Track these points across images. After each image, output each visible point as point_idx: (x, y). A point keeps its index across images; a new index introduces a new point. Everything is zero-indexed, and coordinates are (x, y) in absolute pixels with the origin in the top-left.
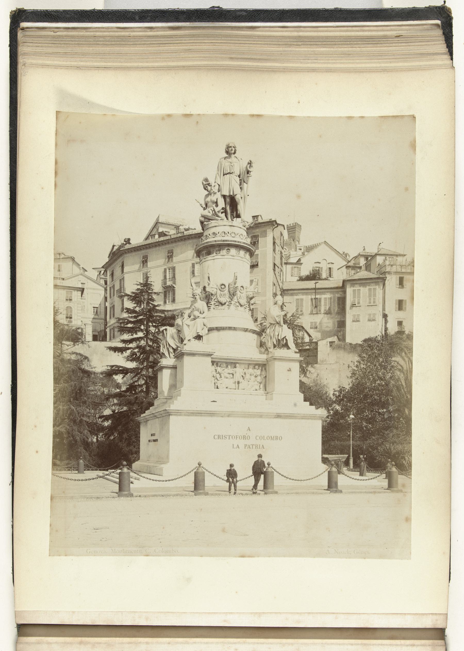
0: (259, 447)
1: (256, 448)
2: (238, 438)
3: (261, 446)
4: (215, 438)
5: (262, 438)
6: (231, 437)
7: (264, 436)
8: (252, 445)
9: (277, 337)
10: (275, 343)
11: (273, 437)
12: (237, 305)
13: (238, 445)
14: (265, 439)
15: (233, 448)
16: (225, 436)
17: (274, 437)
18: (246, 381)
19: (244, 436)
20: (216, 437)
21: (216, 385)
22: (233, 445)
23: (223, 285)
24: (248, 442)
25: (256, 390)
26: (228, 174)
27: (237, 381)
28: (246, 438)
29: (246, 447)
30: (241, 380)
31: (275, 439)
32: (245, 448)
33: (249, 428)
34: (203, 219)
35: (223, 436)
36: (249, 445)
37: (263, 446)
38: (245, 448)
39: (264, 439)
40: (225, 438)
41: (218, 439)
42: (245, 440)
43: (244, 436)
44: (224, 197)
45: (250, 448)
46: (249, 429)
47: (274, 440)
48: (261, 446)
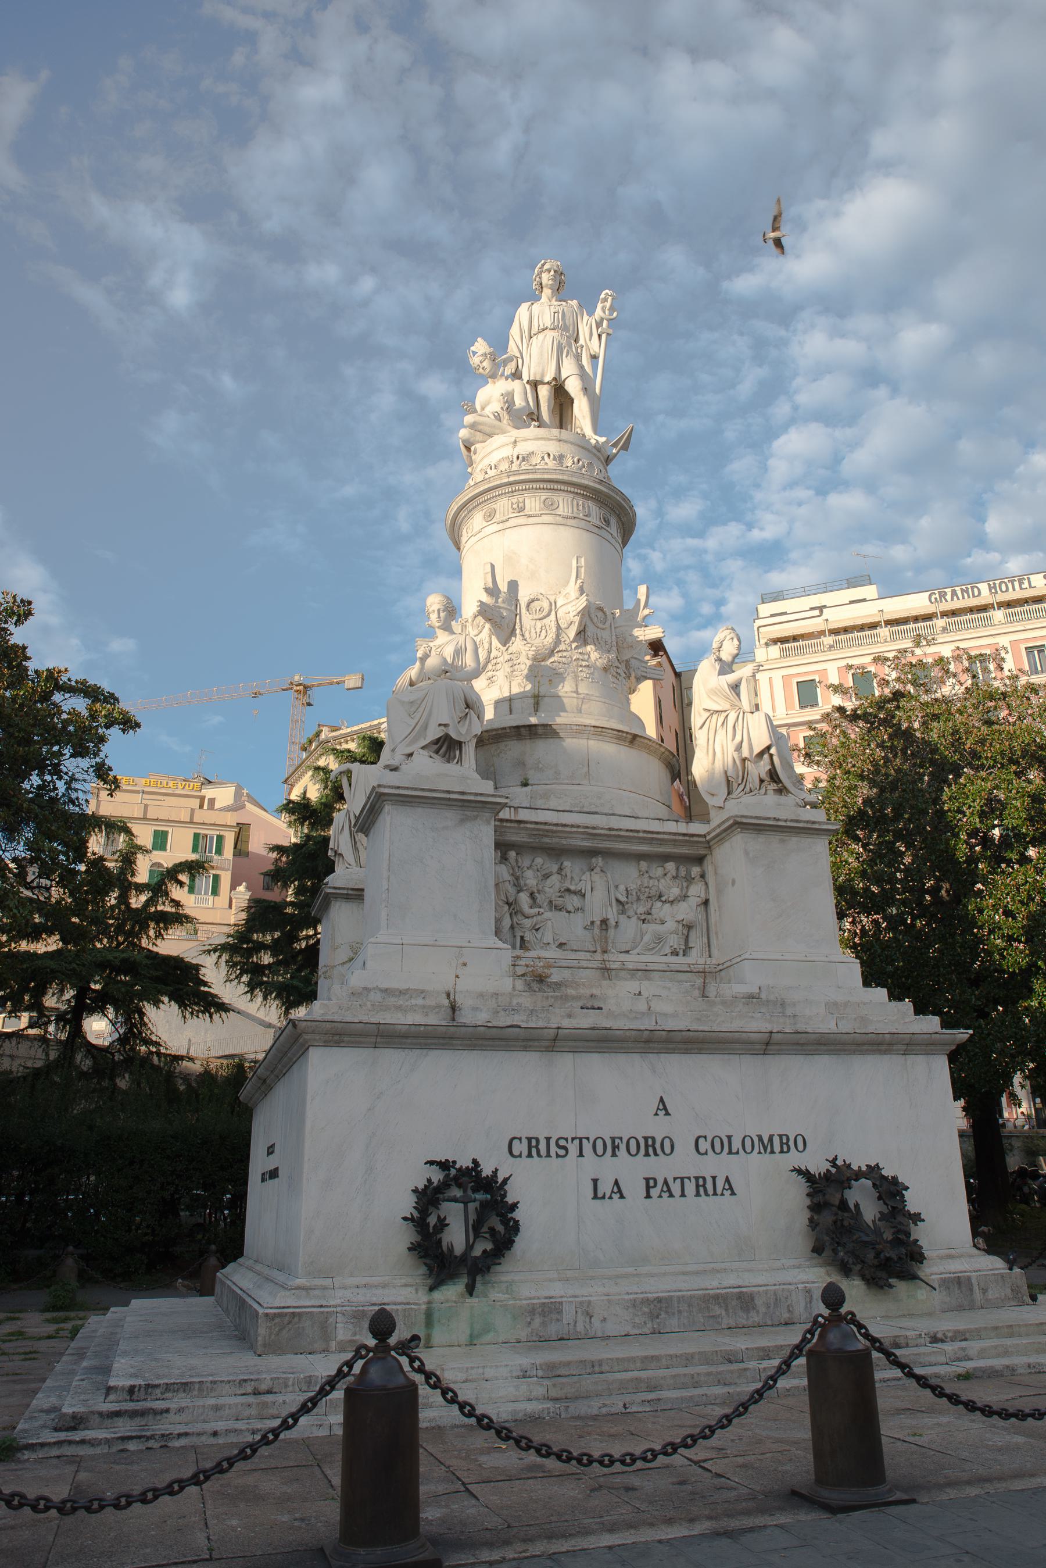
0: (710, 1191)
1: (698, 1194)
2: (622, 1151)
4: (516, 1152)
5: (724, 1145)
6: (587, 1147)
7: (729, 1137)
8: (682, 1179)
13: (616, 1183)
14: (734, 1150)
15: (595, 1197)
16: (562, 1143)
18: (634, 919)
19: (646, 1139)
20: (520, 1147)
21: (519, 934)
22: (595, 1181)
24: (661, 1167)
25: (675, 953)
28: (658, 1146)
29: (654, 1192)
30: (612, 915)
31: (777, 1148)
32: (648, 1196)
33: (662, 1100)
35: (553, 1143)
36: (666, 1182)
37: (727, 1180)
38: (648, 1196)
39: (730, 1152)
40: (562, 1152)
41: (530, 1155)
43: (646, 1139)
44: (535, 384)
45: (671, 1195)
46: (663, 1107)
47: (772, 1152)
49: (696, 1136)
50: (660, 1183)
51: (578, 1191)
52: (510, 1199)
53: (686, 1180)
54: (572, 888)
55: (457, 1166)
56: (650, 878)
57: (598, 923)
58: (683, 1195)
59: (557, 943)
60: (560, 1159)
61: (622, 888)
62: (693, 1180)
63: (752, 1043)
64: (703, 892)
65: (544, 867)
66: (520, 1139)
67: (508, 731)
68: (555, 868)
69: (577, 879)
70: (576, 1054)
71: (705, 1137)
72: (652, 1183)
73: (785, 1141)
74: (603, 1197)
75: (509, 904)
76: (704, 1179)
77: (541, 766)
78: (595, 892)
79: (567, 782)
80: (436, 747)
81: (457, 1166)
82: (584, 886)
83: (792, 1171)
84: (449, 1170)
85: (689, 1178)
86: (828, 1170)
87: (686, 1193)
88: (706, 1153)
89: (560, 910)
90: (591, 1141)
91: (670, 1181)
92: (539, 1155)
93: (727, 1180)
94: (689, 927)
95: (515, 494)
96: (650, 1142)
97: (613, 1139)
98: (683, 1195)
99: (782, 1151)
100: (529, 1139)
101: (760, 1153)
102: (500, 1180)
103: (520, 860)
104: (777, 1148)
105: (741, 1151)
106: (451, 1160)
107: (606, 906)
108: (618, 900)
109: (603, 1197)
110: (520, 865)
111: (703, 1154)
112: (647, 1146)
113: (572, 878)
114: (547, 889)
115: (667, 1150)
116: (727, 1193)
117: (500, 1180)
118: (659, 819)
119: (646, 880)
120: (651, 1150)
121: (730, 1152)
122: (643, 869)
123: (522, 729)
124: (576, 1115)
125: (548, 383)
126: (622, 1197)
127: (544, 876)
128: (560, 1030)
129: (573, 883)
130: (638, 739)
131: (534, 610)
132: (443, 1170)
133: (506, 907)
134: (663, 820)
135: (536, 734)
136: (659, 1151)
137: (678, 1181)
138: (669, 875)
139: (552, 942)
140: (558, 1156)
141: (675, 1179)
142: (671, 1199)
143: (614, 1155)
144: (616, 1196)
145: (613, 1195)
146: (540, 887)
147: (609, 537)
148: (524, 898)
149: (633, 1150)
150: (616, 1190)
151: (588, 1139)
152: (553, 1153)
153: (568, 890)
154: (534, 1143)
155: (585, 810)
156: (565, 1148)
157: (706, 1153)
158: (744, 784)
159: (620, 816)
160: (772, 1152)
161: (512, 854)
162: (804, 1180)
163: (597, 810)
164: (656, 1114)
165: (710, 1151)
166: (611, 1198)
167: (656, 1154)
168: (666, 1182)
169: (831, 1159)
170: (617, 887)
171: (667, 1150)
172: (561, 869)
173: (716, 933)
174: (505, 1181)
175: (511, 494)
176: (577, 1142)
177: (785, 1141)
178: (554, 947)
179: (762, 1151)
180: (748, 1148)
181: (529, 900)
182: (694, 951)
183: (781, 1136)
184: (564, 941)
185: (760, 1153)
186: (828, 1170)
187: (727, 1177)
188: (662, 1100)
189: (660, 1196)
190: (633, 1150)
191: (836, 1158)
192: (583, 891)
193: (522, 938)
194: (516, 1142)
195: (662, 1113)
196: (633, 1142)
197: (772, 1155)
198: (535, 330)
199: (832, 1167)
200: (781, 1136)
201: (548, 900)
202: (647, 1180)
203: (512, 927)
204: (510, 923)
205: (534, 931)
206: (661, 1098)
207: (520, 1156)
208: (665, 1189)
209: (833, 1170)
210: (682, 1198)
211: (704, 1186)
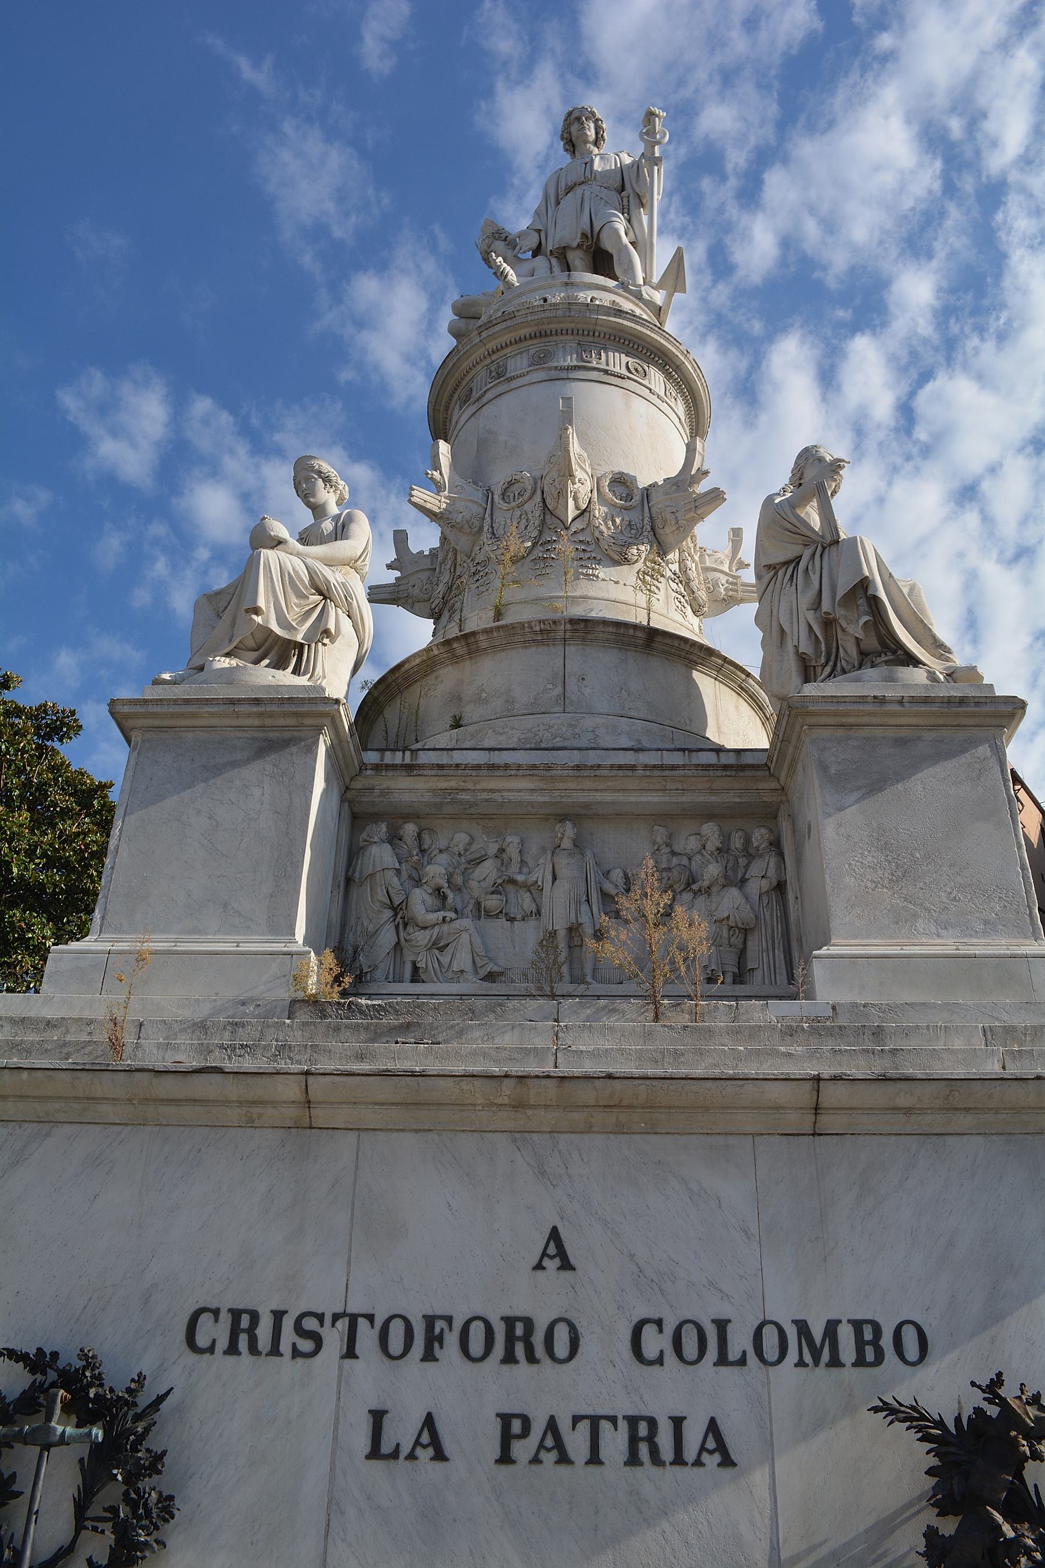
0: (667, 1452)
1: (633, 1460)
3: (694, 1435)
4: (202, 1341)
6: (367, 1337)
7: (721, 1325)
8: (595, 1421)
9: (811, 616)
10: (805, 647)
11: (817, 1332)
12: (587, 555)
13: (429, 1421)
14: (733, 1355)
15: (375, 1453)
16: (310, 1324)
17: (831, 1328)
19: (509, 1322)
21: (409, 957)
22: (378, 1417)
23: (510, 484)
26: (570, 189)
27: (560, 926)
29: (521, 1450)
31: (848, 1351)
33: (554, 1235)
34: (462, 324)
35: (288, 1323)
36: (552, 1425)
37: (713, 1427)
38: (505, 1458)
39: (722, 1360)
40: (306, 1346)
41: (232, 1349)
42: (523, 1368)
45: (564, 1459)
47: (835, 1362)
48: (694, 1435)
49: (635, 1320)
50: (538, 1427)
51: (335, 1439)
52: (155, 1443)
53: (605, 1426)
54: (520, 878)
55: (61, 1364)
56: (674, 853)
57: (562, 934)
58: (594, 1459)
59: (483, 972)
60: (300, 1361)
61: (617, 875)
62: (623, 1425)
63: (778, 1108)
64: (772, 865)
65: (473, 848)
66: (216, 1312)
67: (436, 652)
68: (493, 849)
69: (531, 863)
70: (363, 1135)
71: (659, 1323)
72: (516, 1426)
73: (868, 1334)
74: (395, 1455)
75: (395, 909)
76: (652, 1422)
77: (484, 695)
78: (557, 882)
79: (521, 712)
80: (255, 655)
81: (61, 1364)
82: (541, 874)
83: (875, 1410)
84: (44, 1373)
85: (613, 1420)
86: (978, 1411)
87: (603, 1454)
88: (660, 1361)
89: (497, 916)
90: (379, 1323)
91: (564, 1425)
92: (253, 1349)
93: (713, 1427)
94: (746, 932)
95: (494, 358)
96: (519, 1330)
97: (430, 1321)
98: (594, 1459)
99: (860, 1362)
100: (236, 1314)
101: (801, 1363)
102: (144, 1400)
103: (426, 836)
104: (848, 1351)
105: (752, 1357)
106: (47, 1351)
107: (578, 903)
108: (604, 895)
109: (395, 1455)
110: (426, 847)
111: (651, 1363)
112: (510, 1339)
113: (523, 862)
114: (473, 884)
115: (561, 1349)
116: (712, 1460)
117: (144, 1400)
118: (683, 750)
119: (664, 858)
120: (519, 1350)
121: (722, 1360)
122: (658, 839)
123: (455, 645)
124: (349, 1263)
125: (579, 246)
126: (440, 1456)
127: (469, 862)
128: (311, 1080)
129: (525, 870)
130: (659, 639)
131: (512, 495)
132: (32, 1372)
133: (391, 913)
134: (690, 751)
135: (478, 650)
136: (540, 1351)
137: (584, 1426)
138: (710, 847)
139: (468, 967)
140: (296, 1353)
141: (576, 1419)
142: (563, 1470)
143: (429, 1356)
144: (425, 1455)
145: (419, 1452)
146: (459, 880)
147: (646, 392)
148: (420, 902)
149: (476, 1347)
150: (425, 1438)
151: (370, 1318)
152: (285, 1347)
153: (512, 882)
154: (245, 1321)
155: (543, 745)
156: (317, 1339)
157: (660, 1361)
158: (831, 663)
159: (607, 749)
160: (835, 1362)
161: (410, 829)
162: (913, 1435)
163: (567, 744)
164: (539, 1267)
165: (670, 1358)
166: (412, 1456)
167: (531, 1359)
168: (552, 1425)
169: (984, 1382)
170: (607, 874)
171: (561, 1349)
172: (502, 850)
173: (800, 940)
174: (161, 1399)
175: (488, 361)
176: (343, 1324)
177: (868, 1335)
178: (470, 976)
179: (808, 1358)
180: (771, 1350)
181: (429, 900)
182: (758, 975)
183: (857, 1325)
184: (496, 969)
185: (801, 1363)
186: (978, 1411)
187: (713, 1421)
188: (554, 1235)
189: (536, 1460)
190: (476, 1347)
191: (998, 1381)
192: (540, 883)
193: (414, 963)
194: (205, 1319)
195: (551, 1265)
196: (477, 1330)
197: (834, 1371)
198: (561, 192)
199: (990, 1401)
200: (857, 1325)
201: (472, 901)
202: (506, 1419)
203: (398, 946)
204: (394, 940)
205: (436, 952)
206: (554, 1231)
207: (211, 1350)
208: (549, 1442)
209: (993, 1411)
210: (591, 1468)
211: (651, 1439)
